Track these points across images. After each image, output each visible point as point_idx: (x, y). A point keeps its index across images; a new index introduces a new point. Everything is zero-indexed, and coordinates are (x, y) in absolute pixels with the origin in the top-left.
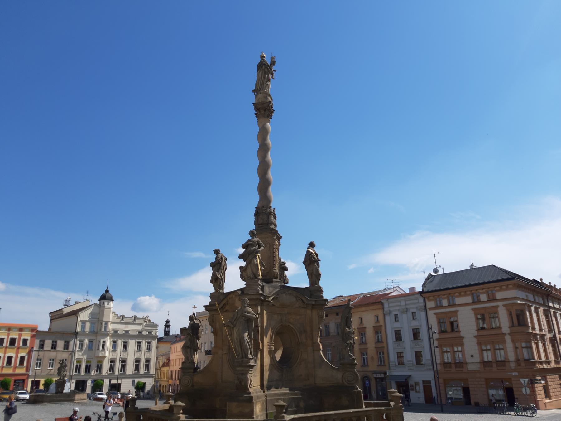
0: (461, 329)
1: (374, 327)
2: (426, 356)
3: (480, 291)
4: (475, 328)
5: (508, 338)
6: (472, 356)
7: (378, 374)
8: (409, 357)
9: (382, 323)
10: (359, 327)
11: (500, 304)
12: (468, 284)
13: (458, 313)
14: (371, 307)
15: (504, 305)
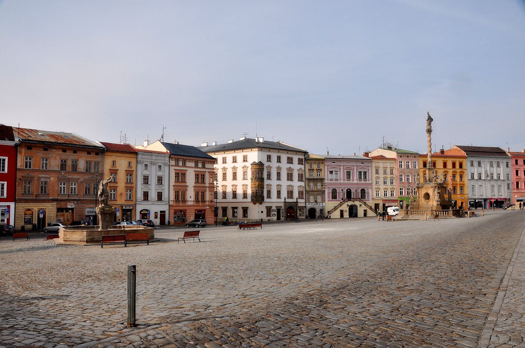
0: (187, 181)
1: (126, 170)
2: (165, 196)
3: (199, 161)
4: (194, 181)
5: (207, 189)
6: (191, 197)
7: (127, 207)
8: (153, 195)
9: (134, 168)
10: (111, 168)
11: (207, 170)
12: (197, 156)
13: (187, 172)
14: (126, 155)
15: (209, 172)
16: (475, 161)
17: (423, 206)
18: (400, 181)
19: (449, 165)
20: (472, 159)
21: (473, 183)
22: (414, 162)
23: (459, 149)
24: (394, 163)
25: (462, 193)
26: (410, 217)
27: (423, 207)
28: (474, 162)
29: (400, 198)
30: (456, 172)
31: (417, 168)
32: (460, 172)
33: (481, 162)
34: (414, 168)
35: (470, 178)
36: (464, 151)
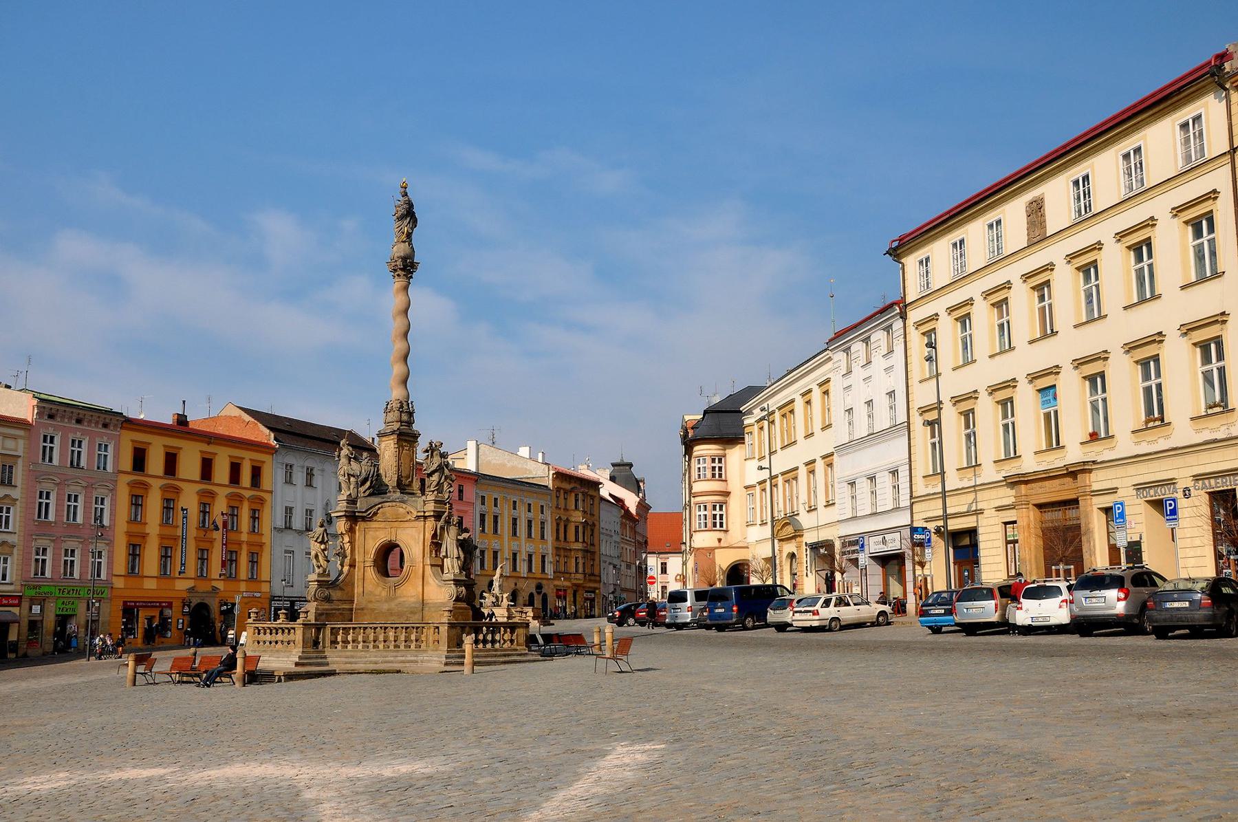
16: (300, 463)
17: (370, 606)
18: (39, 516)
19: (221, 473)
20: (290, 459)
21: (289, 539)
22: (100, 445)
23: (247, 418)
24: (21, 437)
25: (253, 579)
26: (335, 658)
27: (373, 610)
28: (295, 468)
29: (35, 587)
30: (240, 498)
31: (110, 468)
32: (253, 500)
33: (315, 472)
34: (98, 468)
35: (280, 523)
36: (271, 429)
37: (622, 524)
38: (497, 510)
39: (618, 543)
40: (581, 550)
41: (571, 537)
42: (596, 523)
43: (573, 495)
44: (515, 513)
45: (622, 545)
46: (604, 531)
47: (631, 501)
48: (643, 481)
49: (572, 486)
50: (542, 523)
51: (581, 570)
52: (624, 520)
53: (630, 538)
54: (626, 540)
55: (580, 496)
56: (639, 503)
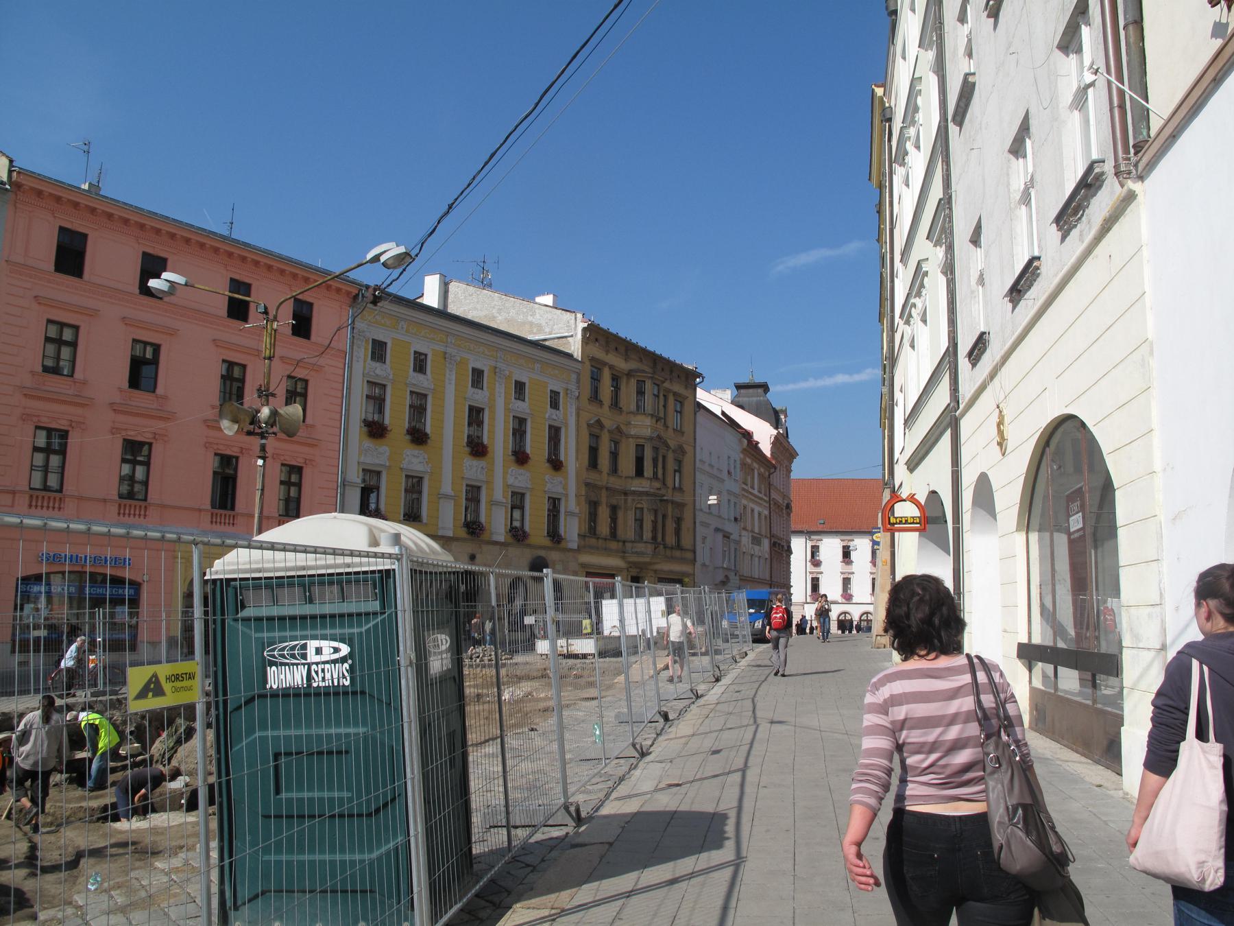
37: (743, 464)
38: (423, 382)
39: (736, 495)
40: (647, 494)
41: (627, 464)
42: (688, 448)
43: (633, 382)
44: (479, 397)
45: (744, 502)
46: (707, 468)
47: (763, 433)
48: (785, 412)
49: (633, 365)
50: (555, 434)
51: (647, 535)
52: (749, 460)
53: (760, 492)
54: (751, 493)
55: (649, 387)
56: (776, 437)
